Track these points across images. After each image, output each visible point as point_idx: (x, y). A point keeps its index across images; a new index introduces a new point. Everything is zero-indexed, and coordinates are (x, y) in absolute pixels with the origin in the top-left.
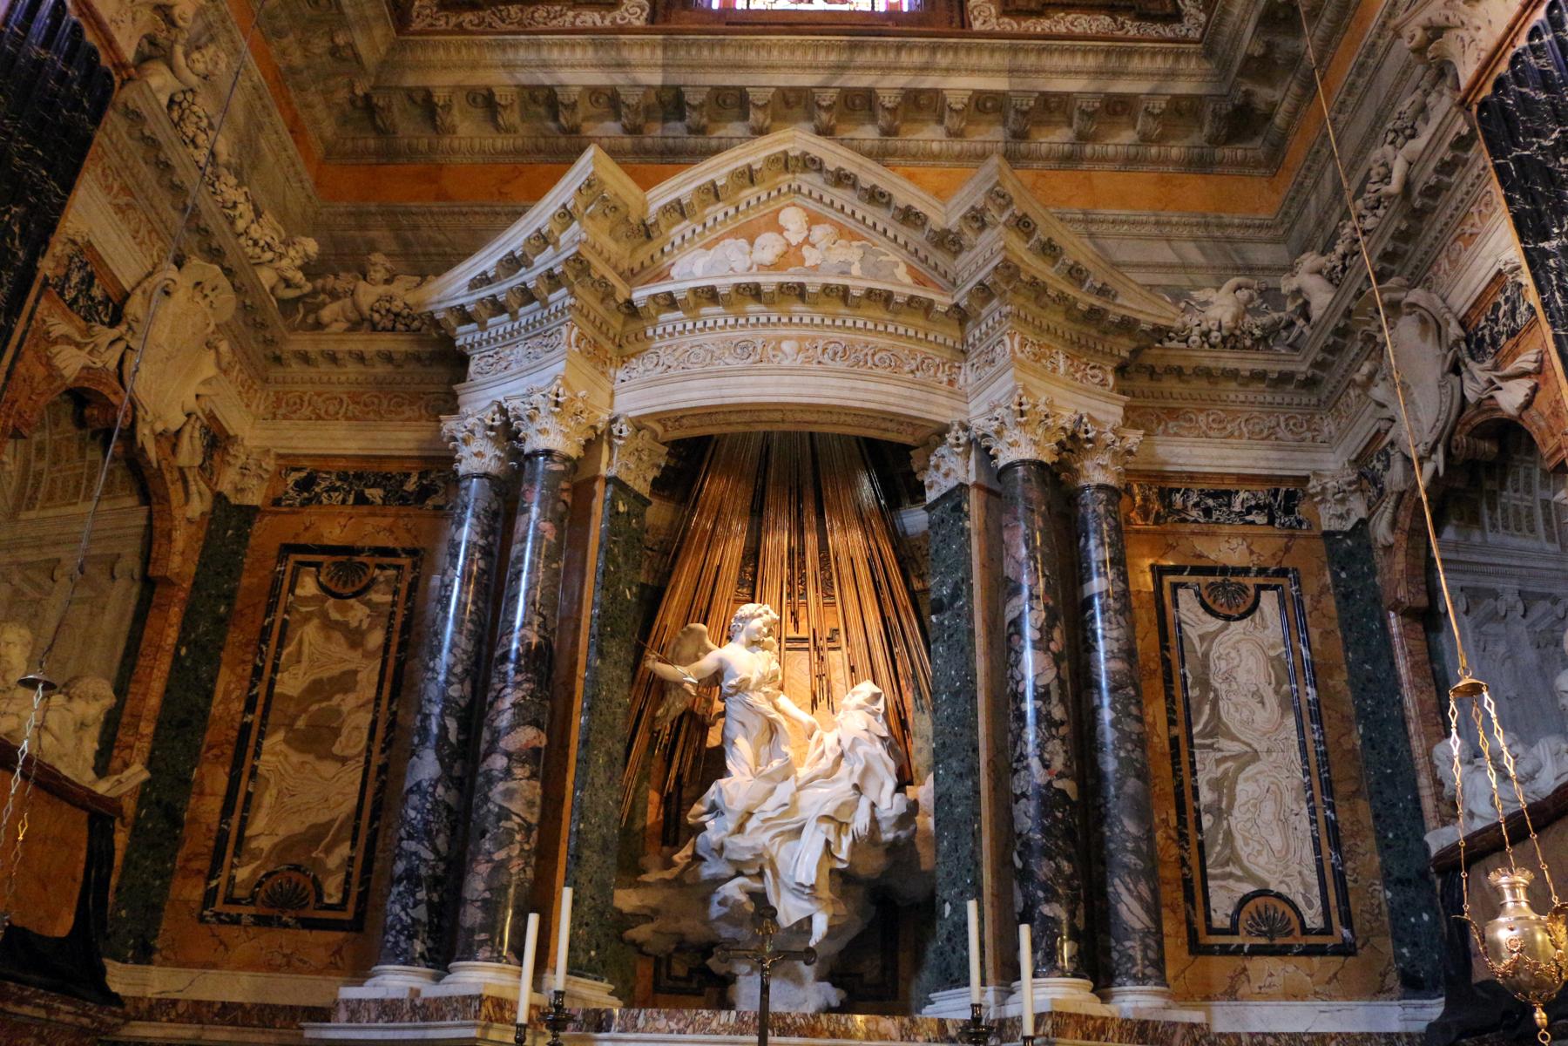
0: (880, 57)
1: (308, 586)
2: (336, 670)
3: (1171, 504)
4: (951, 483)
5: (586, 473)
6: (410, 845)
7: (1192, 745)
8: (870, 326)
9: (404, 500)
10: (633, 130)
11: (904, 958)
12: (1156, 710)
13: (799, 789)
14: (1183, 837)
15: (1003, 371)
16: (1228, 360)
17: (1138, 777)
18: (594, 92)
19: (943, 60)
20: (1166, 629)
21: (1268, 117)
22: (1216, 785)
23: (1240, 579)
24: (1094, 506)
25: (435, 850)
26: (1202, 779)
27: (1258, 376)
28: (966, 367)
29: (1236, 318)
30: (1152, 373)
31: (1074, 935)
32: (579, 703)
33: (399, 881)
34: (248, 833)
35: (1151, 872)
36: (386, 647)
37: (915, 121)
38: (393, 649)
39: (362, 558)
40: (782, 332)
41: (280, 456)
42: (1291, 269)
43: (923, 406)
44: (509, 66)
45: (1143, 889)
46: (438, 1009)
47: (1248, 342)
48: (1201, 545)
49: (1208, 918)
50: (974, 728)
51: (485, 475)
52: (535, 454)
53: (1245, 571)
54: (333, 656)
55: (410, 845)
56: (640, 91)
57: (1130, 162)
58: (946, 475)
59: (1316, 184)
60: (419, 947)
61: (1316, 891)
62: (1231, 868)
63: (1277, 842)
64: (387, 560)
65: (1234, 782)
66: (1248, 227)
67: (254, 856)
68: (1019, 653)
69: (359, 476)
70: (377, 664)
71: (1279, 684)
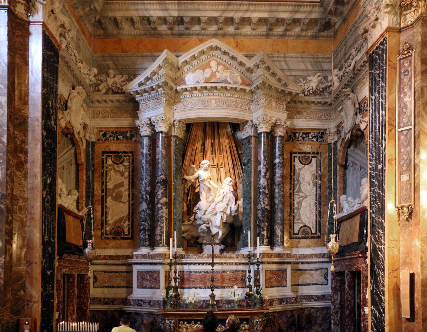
1: (110, 162)
2: (119, 182)
3: (296, 136)
4: (248, 135)
7: (294, 194)
8: (231, 95)
9: (127, 138)
10: (171, 29)
11: (236, 238)
12: (287, 187)
13: (216, 204)
14: (290, 214)
18: (160, 18)
20: (292, 168)
22: (298, 203)
23: (308, 155)
26: (295, 202)
27: (319, 103)
28: (253, 104)
29: (318, 86)
30: (295, 102)
32: (173, 190)
33: (142, 230)
36: (129, 176)
37: (243, 25)
38: (131, 176)
40: (212, 97)
41: (97, 128)
43: (243, 116)
44: (136, 10)
45: (281, 228)
46: (154, 256)
47: (319, 92)
48: (301, 147)
49: (294, 231)
50: (251, 194)
51: (148, 136)
53: (310, 153)
54: (119, 179)
55: (143, 223)
56: (172, 18)
58: (247, 133)
59: (341, 51)
60: (147, 243)
61: (315, 225)
62: (299, 221)
63: (308, 215)
64: (126, 154)
65: (302, 203)
66: (324, 58)
68: (260, 178)
69: (116, 133)
70: (128, 180)
71: (313, 180)
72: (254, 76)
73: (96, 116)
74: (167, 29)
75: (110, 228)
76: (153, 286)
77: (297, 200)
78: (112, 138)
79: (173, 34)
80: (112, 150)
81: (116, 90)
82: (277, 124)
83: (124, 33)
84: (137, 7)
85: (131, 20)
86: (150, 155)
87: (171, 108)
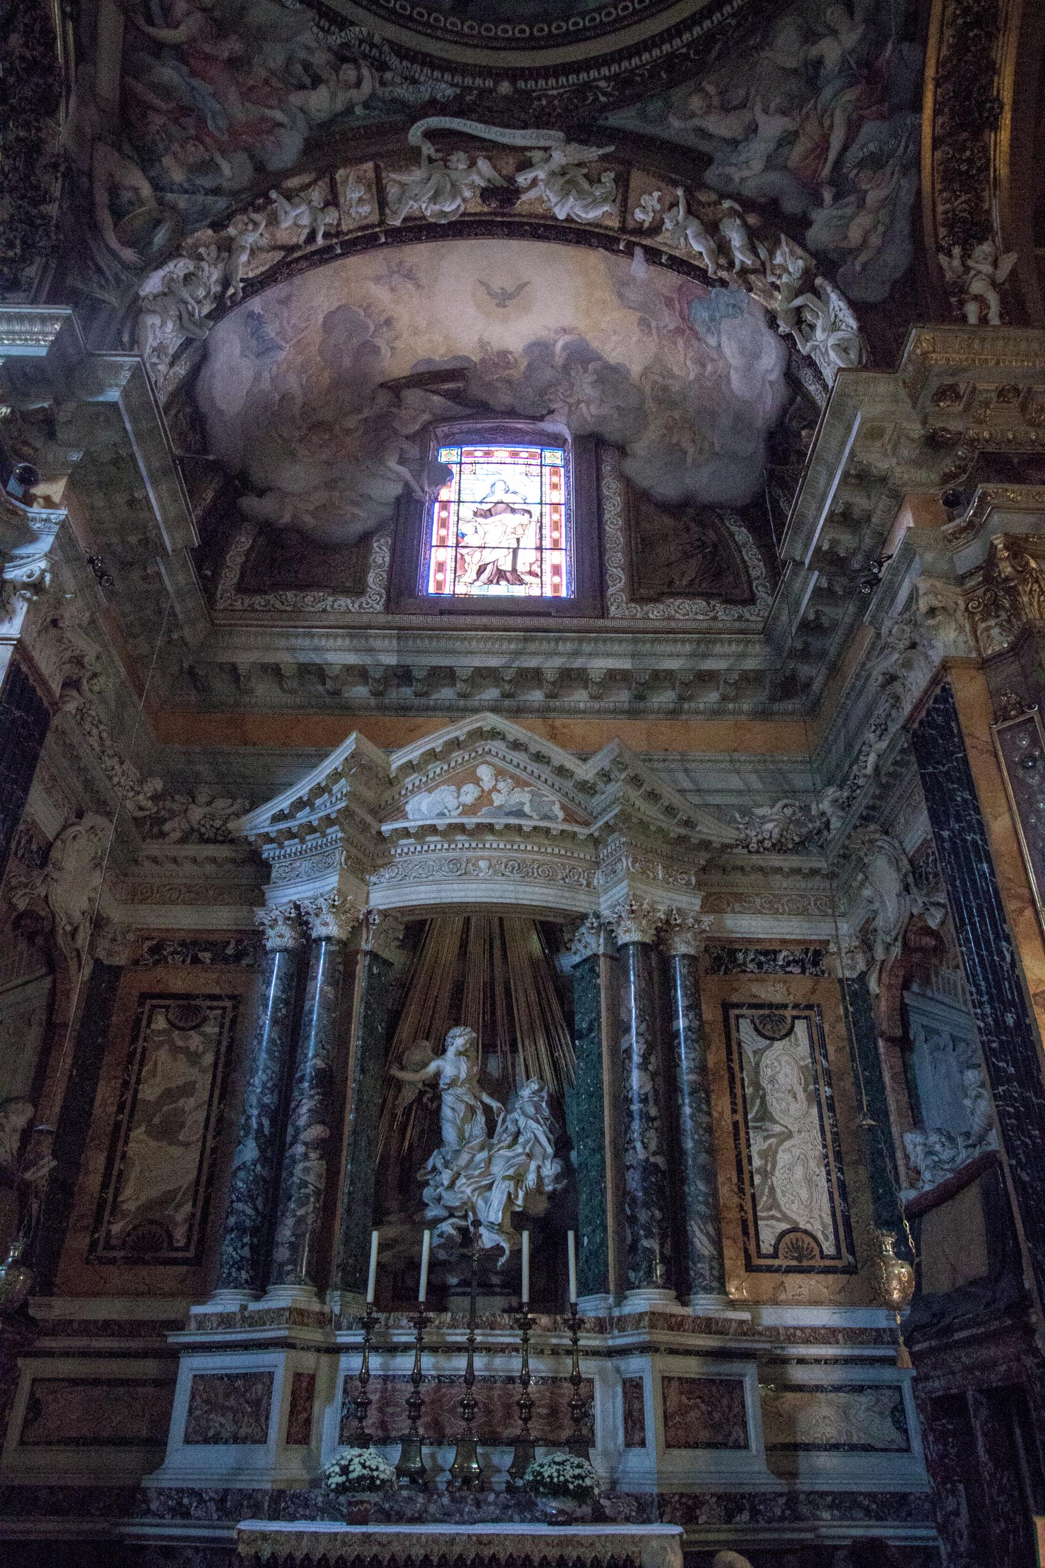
0: (545, 646)
1: (160, 1023)
2: (181, 1082)
3: (736, 960)
4: (589, 953)
5: (352, 947)
6: (239, 1206)
7: (747, 1127)
9: (226, 959)
12: (722, 1104)
14: (742, 1191)
15: (621, 881)
16: (775, 860)
17: (707, 1152)
19: (587, 648)
20: (732, 1047)
21: (808, 685)
22: (764, 1154)
23: (781, 1012)
24: (679, 970)
25: (255, 1209)
27: (797, 871)
28: (599, 873)
31: (664, 1260)
32: (351, 1106)
33: (232, 1230)
35: (716, 1217)
36: (216, 1065)
39: (198, 1002)
41: (138, 930)
42: (818, 794)
44: (292, 649)
45: (711, 1229)
47: (790, 846)
49: (758, 1246)
52: (319, 939)
53: (785, 1006)
55: (239, 1206)
56: (382, 669)
57: (716, 713)
60: (244, 1275)
61: (831, 1229)
62: (773, 1212)
64: (215, 1004)
67: (124, 1215)
68: (630, 1072)
69: (194, 943)
70: (209, 1077)
72: (597, 802)
73: (139, 897)
74: (368, 695)
75: (123, 1230)
76: (243, 1432)
77: (758, 1144)
79: (383, 708)
81: (210, 834)
82: (673, 922)
83: (253, 701)
84: (293, 641)
85: (275, 671)
86: (287, 1003)
87: (363, 880)
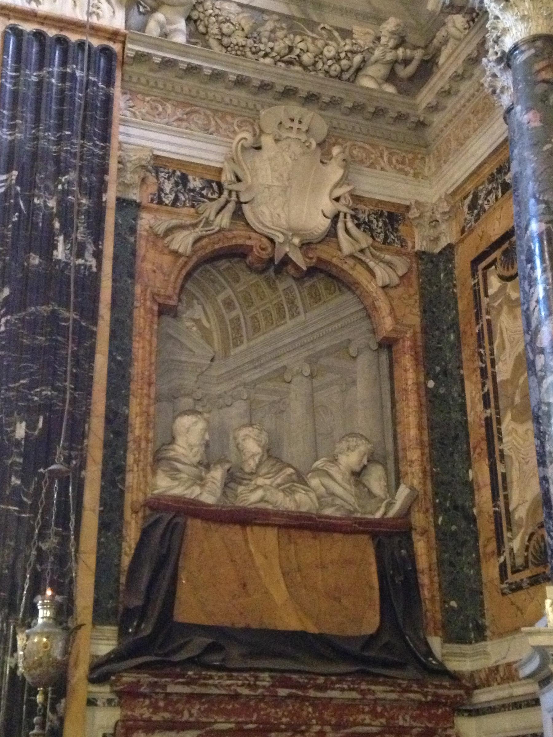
34: (511, 508)
78: (492, 197)
80: (494, 239)
